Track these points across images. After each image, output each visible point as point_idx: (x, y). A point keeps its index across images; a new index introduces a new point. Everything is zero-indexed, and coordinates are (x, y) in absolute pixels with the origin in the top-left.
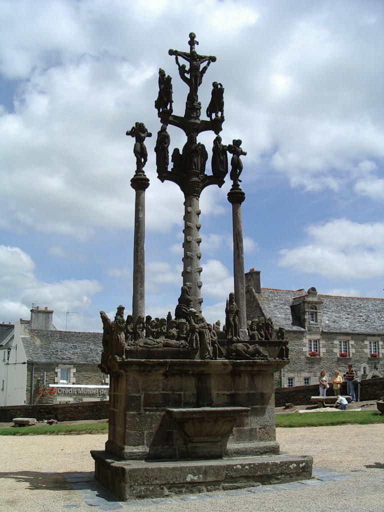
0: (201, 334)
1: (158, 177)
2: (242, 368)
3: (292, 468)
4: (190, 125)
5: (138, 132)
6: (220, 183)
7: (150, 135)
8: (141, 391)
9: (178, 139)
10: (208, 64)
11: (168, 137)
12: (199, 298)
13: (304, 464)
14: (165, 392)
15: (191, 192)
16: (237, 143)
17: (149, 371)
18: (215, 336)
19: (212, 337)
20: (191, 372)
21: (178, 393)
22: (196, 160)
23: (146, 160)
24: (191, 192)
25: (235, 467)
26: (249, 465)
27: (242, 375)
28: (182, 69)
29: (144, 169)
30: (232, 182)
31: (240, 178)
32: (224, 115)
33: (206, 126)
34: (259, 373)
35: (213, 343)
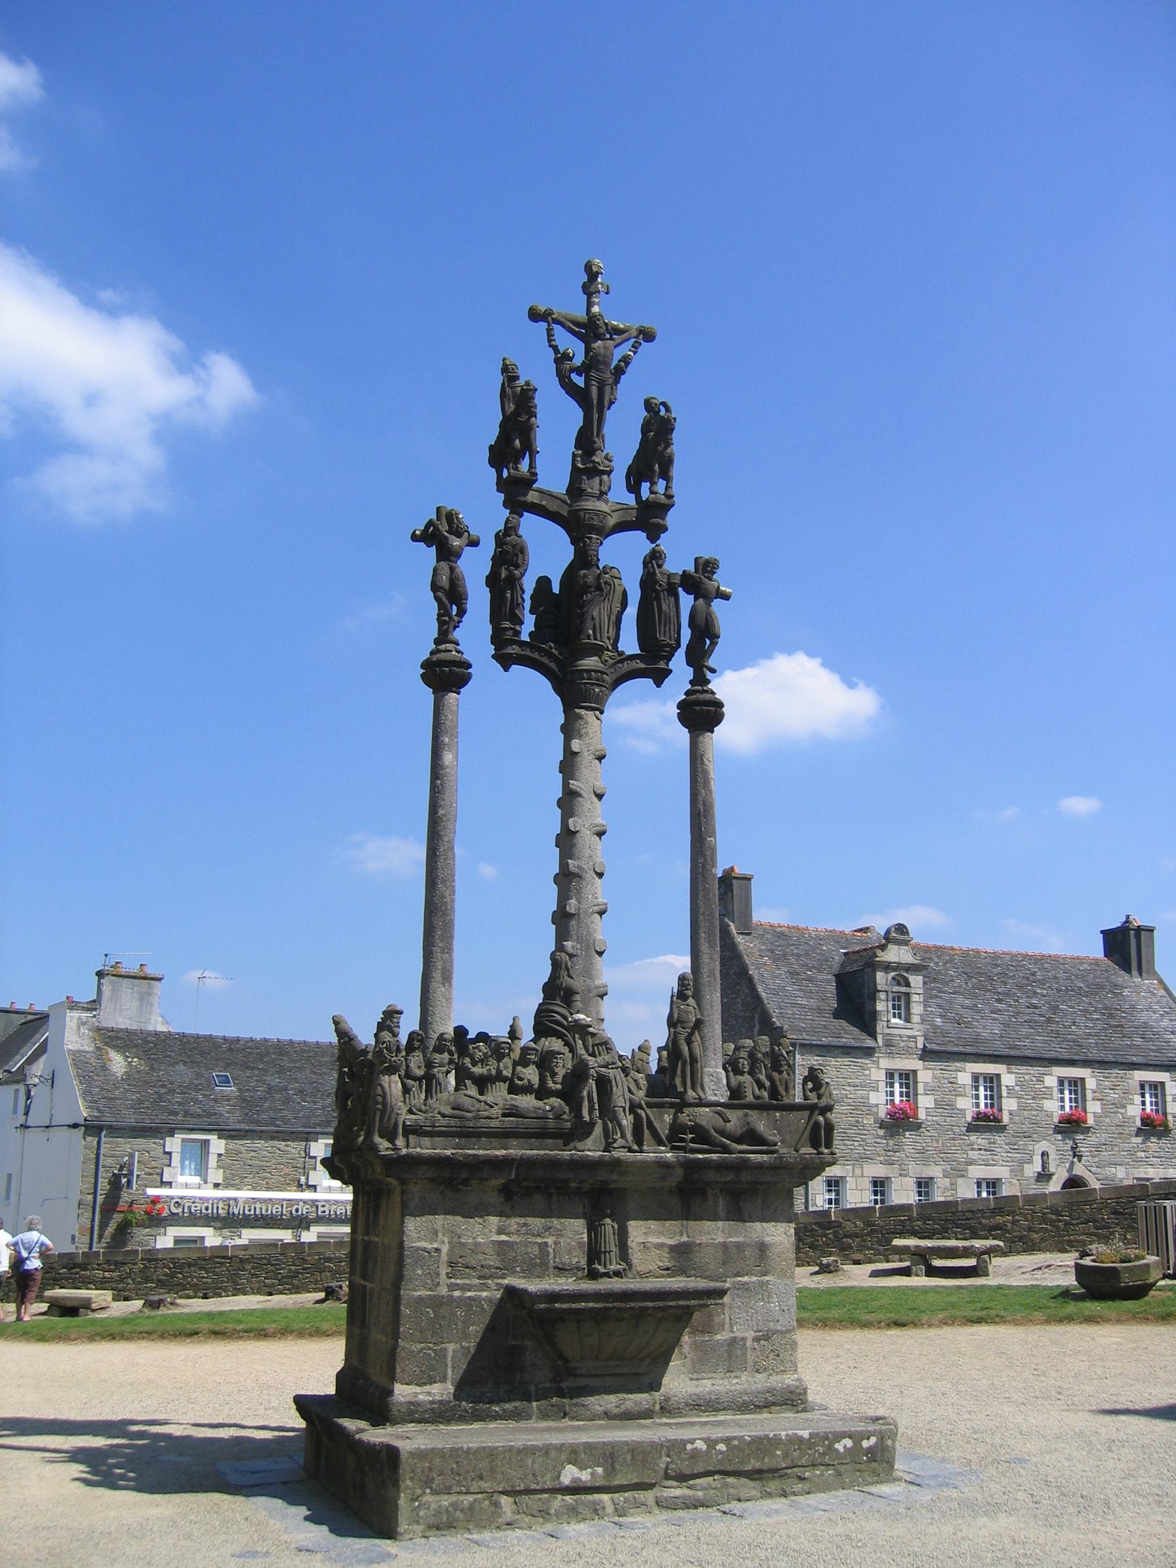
0: (603, 1084)
1: (493, 657)
2: (710, 1176)
3: (842, 1450)
5: (443, 535)
7: (474, 543)
8: (440, 1235)
9: (548, 553)
10: (635, 347)
11: (522, 550)
12: (598, 982)
13: (873, 1440)
14: (504, 1238)
15: (578, 695)
16: (707, 567)
17: (466, 1182)
18: (639, 1088)
19: (630, 1091)
20: (573, 1185)
21: (539, 1240)
22: (595, 614)
23: (462, 612)
24: (578, 695)
25: (689, 1447)
26: (727, 1440)
27: (710, 1191)
29: (457, 634)
30: (689, 673)
31: (711, 662)
32: (675, 491)
34: (753, 1189)
35: (634, 1107)
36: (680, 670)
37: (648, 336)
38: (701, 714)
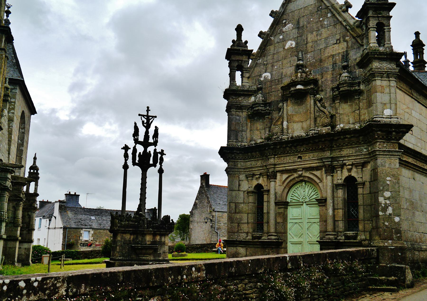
0: (143, 221)
4: (146, 144)
5: (126, 148)
6: (155, 166)
7: (130, 149)
9: (140, 149)
16: (162, 151)
28: (143, 122)
30: (160, 166)
33: (151, 144)
36: (158, 165)
37: (156, 117)
38: (161, 171)
